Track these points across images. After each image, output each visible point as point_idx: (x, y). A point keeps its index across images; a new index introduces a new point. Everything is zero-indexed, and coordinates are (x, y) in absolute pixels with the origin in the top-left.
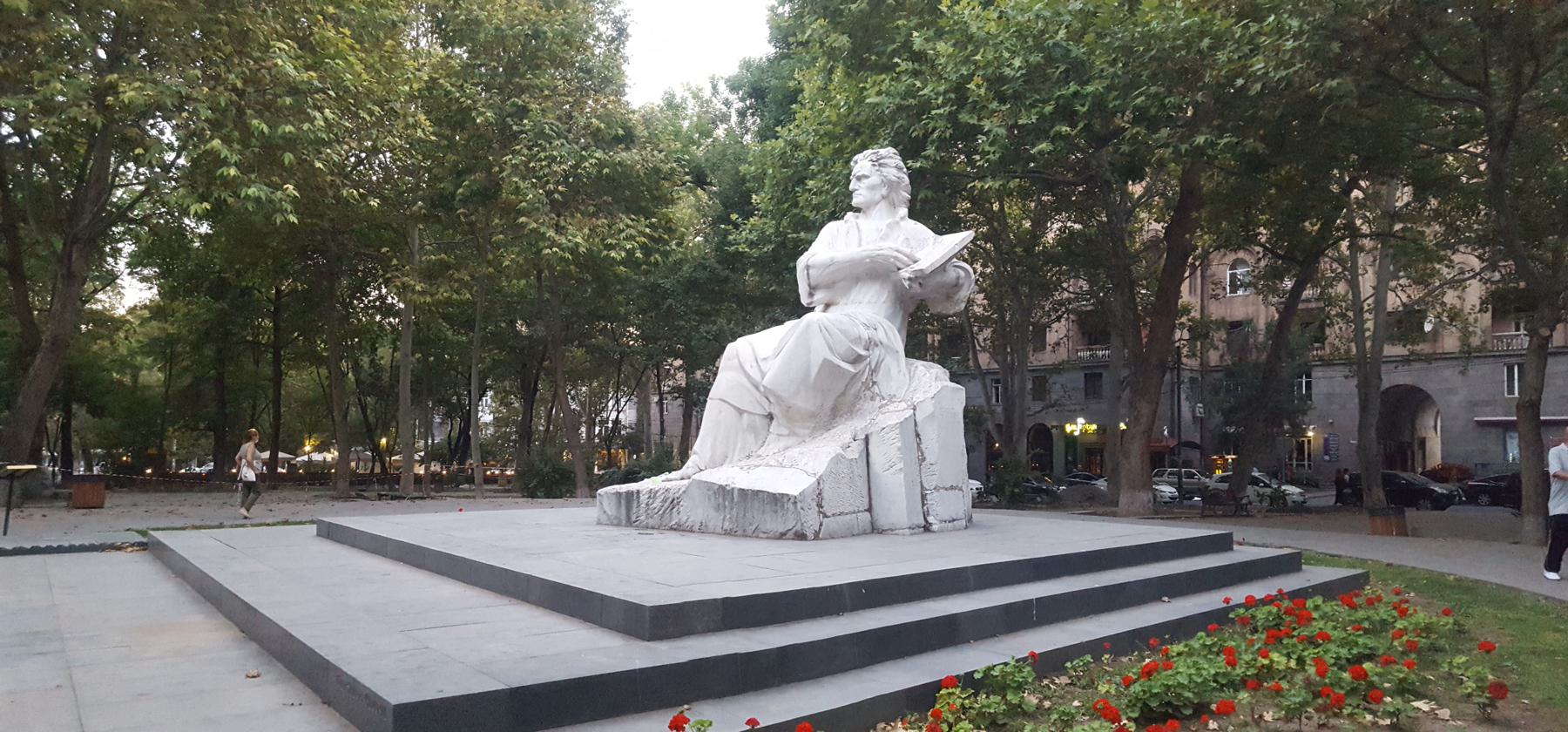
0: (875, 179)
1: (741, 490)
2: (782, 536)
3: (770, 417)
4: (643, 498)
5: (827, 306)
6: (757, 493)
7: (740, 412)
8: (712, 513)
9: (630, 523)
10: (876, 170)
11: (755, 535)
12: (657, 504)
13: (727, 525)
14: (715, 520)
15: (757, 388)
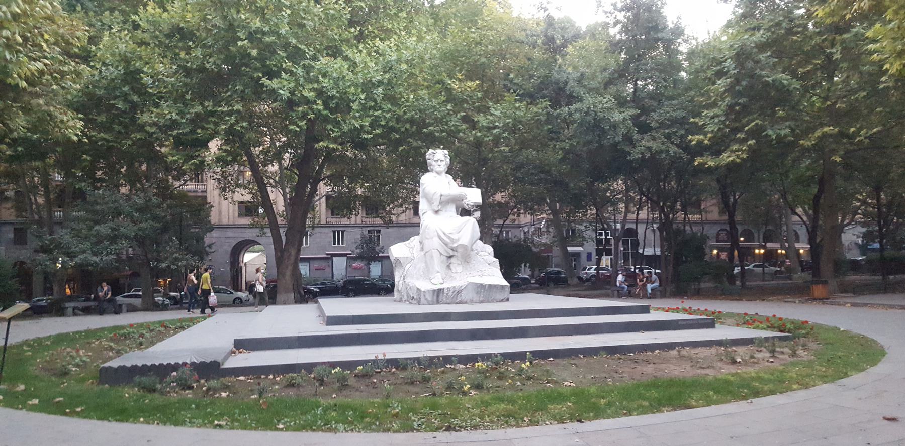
0: (444, 163)
1: (490, 286)
2: (502, 301)
3: (450, 257)
4: (446, 291)
5: (437, 212)
6: (495, 286)
7: (441, 254)
8: (475, 295)
9: (438, 302)
10: (439, 157)
11: (492, 302)
12: (450, 294)
13: (481, 299)
14: (476, 299)
15: (446, 245)
